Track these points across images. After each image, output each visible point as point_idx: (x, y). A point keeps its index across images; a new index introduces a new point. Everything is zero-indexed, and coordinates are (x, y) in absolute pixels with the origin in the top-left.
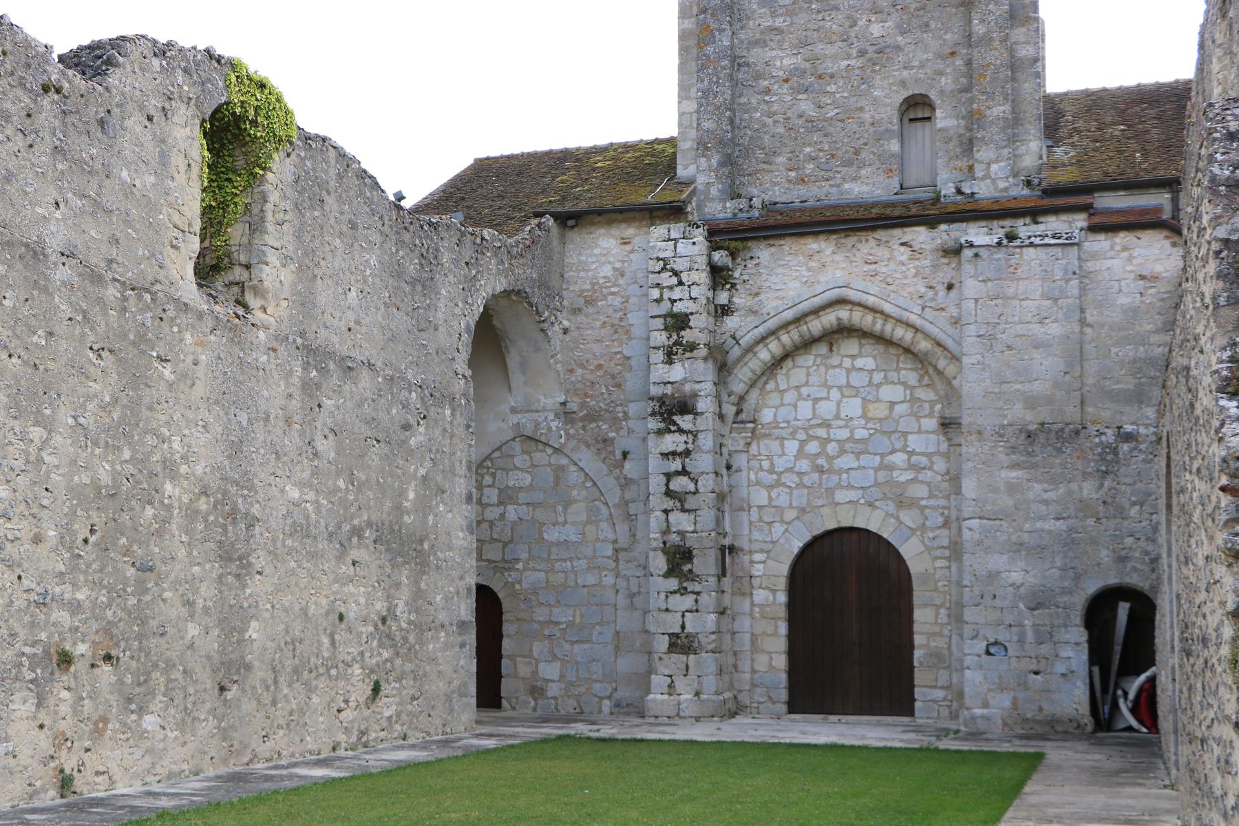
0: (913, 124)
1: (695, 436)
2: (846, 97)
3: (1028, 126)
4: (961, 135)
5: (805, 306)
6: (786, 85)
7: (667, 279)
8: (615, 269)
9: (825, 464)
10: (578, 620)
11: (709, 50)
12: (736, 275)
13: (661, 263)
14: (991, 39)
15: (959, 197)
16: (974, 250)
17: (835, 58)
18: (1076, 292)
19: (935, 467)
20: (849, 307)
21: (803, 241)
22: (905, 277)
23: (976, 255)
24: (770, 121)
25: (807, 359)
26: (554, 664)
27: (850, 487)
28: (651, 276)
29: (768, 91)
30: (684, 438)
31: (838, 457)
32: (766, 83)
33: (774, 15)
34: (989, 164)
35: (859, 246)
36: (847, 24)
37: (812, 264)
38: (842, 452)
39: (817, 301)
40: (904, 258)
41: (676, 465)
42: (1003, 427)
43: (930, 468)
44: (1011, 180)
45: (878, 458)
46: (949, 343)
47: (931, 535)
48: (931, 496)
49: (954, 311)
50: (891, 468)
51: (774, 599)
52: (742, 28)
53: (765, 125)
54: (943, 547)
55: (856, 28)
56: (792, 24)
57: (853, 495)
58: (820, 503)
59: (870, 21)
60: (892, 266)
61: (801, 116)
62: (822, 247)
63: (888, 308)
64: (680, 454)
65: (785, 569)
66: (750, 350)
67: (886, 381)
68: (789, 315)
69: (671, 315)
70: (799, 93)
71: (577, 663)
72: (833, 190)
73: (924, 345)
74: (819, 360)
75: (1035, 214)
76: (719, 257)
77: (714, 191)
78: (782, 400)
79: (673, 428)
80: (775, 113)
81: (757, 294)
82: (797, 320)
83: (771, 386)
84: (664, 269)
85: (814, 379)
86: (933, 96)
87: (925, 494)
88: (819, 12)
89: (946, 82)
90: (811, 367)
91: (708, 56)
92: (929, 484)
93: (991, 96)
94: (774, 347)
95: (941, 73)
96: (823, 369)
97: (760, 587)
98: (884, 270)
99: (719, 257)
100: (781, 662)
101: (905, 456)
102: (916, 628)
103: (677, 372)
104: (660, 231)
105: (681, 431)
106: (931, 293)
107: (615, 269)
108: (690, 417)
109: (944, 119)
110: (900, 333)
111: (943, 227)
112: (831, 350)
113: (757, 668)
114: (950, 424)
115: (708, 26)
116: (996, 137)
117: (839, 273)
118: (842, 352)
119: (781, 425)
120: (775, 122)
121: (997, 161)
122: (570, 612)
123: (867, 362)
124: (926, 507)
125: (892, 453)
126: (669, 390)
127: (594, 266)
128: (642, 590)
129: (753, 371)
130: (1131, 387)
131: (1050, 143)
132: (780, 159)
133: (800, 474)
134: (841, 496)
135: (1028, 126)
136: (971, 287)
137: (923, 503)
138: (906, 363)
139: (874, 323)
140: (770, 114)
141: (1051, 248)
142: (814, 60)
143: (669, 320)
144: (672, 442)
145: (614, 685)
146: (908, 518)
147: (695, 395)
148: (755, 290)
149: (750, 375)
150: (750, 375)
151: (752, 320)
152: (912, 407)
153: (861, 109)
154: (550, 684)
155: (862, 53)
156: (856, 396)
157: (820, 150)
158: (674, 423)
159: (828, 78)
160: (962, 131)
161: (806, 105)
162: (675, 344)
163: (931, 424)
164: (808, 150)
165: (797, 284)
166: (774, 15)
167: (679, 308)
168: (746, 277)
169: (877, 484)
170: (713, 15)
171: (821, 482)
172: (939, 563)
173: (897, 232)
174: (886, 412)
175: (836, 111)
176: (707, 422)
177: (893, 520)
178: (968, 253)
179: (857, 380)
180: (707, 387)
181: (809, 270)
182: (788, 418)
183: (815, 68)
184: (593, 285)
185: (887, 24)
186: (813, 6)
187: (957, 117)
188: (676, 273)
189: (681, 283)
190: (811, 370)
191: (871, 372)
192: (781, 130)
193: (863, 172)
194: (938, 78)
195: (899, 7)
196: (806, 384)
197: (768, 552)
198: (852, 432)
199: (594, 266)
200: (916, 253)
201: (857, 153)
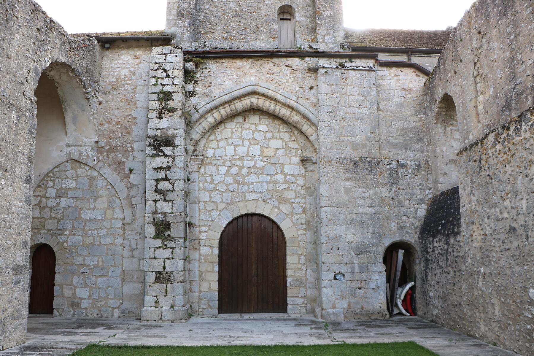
0: (282, 21)
1: (174, 158)
2: (252, 3)
5: (235, 94)
7: (160, 74)
8: (130, 71)
9: (241, 180)
10: (100, 264)
13: (158, 65)
16: (325, 70)
18: (375, 93)
19: (298, 182)
20: (257, 97)
21: (234, 61)
22: (288, 82)
23: (326, 72)
24: (214, 10)
25: (231, 125)
26: (85, 289)
27: (254, 192)
28: (151, 72)
30: (167, 159)
31: (247, 176)
37: (239, 73)
38: (250, 173)
39: (242, 92)
40: (288, 72)
41: (162, 175)
42: (341, 159)
43: (296, 183)
44: (334, 44)
45: (269, 177)
46: (311, 117)
47: (296, 217)
48: (296, 197)
49: (314, 100)
50: (275, 182)
51: (212, 252)
53: (212, 11)
54: (302, 224)
57: (255, 196)
58: (238, 200)
60: (281, 76)
63: (279, 97)
64: (164, 169)
65: (218, 236)
66: (203, 116)
67: (273, 137)
68: (226, 98)
69: (162, 92)
71: (99, 288)
72: (246, 44)
74: (238, 125)
75: (351, 57)
76: (190, 65)
77: (186, 37)
78: (218, 145)
79: (161, 154)
80: (217, 7)
81: (209, 87)
82: (230, 102)
83: (212, 137)
84: (159, 68)
85: (235, 135)
86: (294, 6)
87: (293, 196)
90: (234, 129)
92: (295, 191)
94: (216, 116)
96: (240, 130)
97: (205, 245)
98: (277, 78)
99: (190, 65)
100: (215, 286)
101: (283, 176)
102: (288, 266)
103: (164, 123)
104: (156, 50)
105: (165, 155)
107: (130, 71)
108: (171, 148)
109: (299, 16)
110: (284, 112)
111: (307, 59)
112: (245, 121)
113: (202, 289)
114: (306, 160)
117: (253, 78)
118: (250, 122)
119: (217, 158)
120: (217, 10)
121: (328, 35)
122: (96, 259)
123: (263, 128)
124: (294, 203)
125: (276, 174)
126: (159, 133)
127: (118, 70)
128: (138, 246)
129: (204, 128)
130: (402, 141)
133: (227, 184)
134: (249, 196)
136: (324, 88)
137: (292, 200)
138: (283, 128)
139: (270, 105)
141: (362, 72)
143: (160, 95)
144: (160, 161)
145: (121, 301)
146: (284, 208)
147: (174, 136)
148: (207, 84)
149: (202, 130)
150: (202, 130)
151: (206, 100)
152: (286, 152)
153: (260, 9)
154: (83, 301)
156: (257, 144)
158: (162, 151)
162: (163, 108)
163: (297, 160)
164: (233, 24)
165: (231, 83)
167: (166, 89)
168: (203, 78)
169: (268, 191)
171: (238, 188)
172: (301, 232)
173: (284, 60)
174: (273, 154)
175: (248, 8)
176: (179, 151)
177: (276, 210)
178: (321, 71)
179: (257, 136)
180: (181, 132)
181: (237, 76)
182: (221, 155)
184: (117, 79)
188: (165, 71)
189: (168, 76)
190: (234, 130)
193: (261, 37)
196: (231, 137)
197: (209, 226)
198: (255, 163)
199: (118, 70)
201: (258, 28)
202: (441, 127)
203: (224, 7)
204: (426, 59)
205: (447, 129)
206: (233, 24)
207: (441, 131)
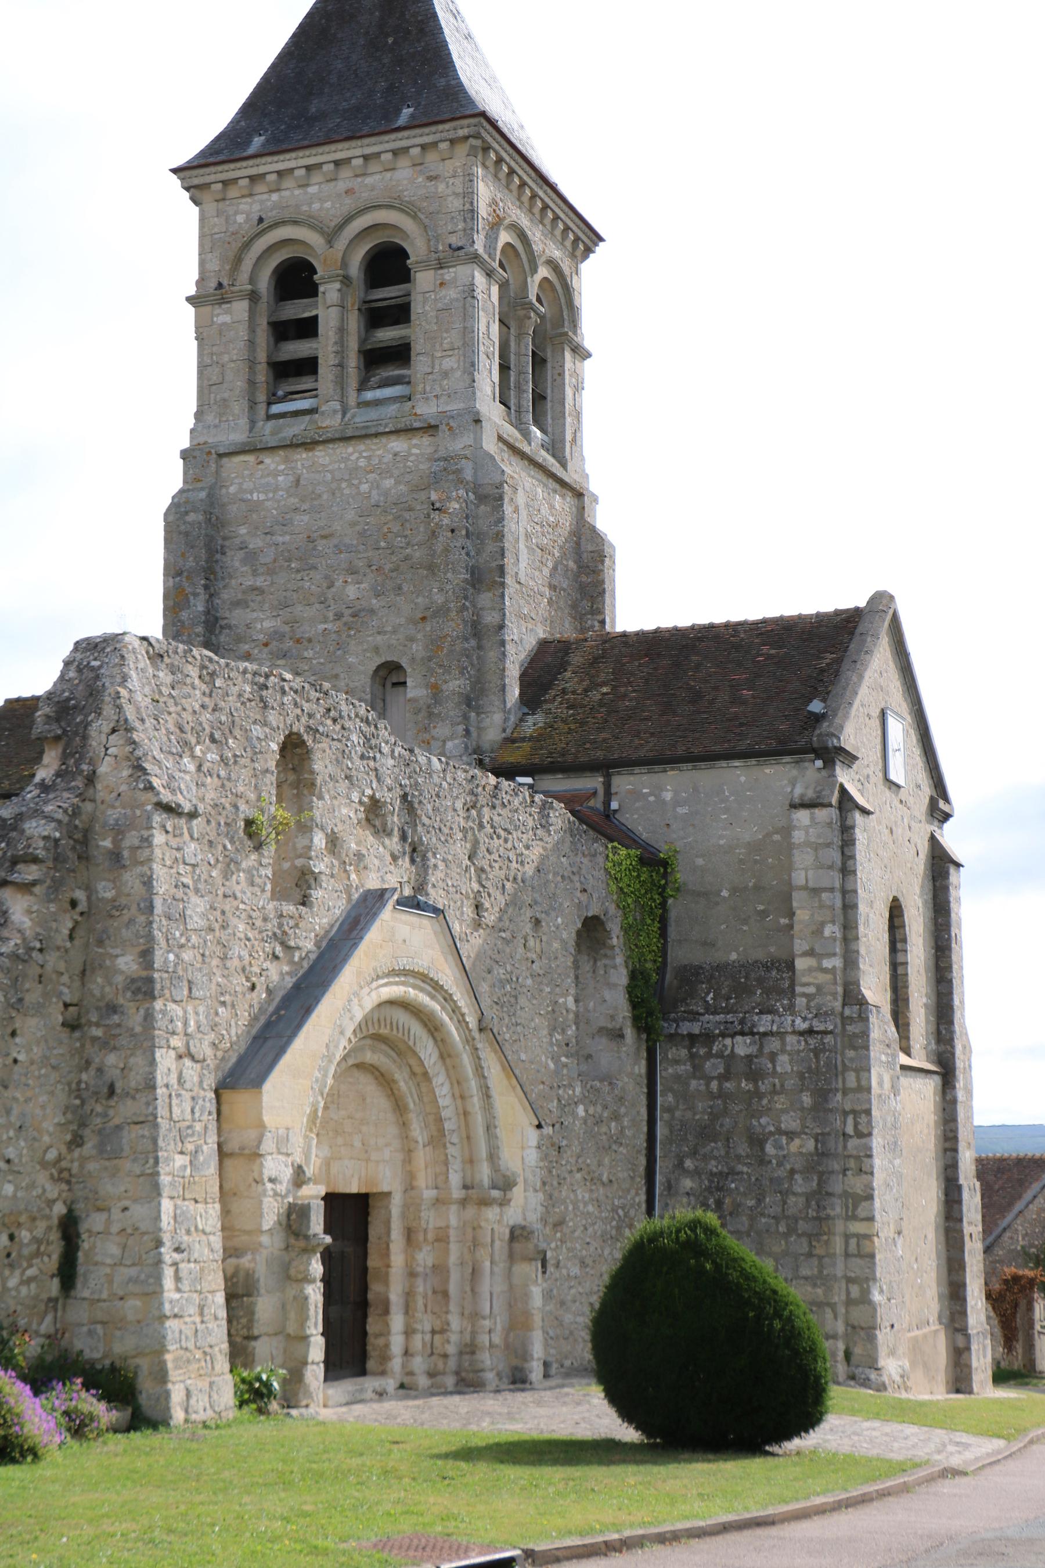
2: (322, 664)
3: (492, 697)
6: (266, 650)
11: (184, 615)
14: (449, 610)
32: (247, 647)
33: (255, 573)
34: (444, 742)
36: (325, 585)
52: (225, 587)
55: (333, 590)
56: (272, 583)
59: (346, 582)
88: (298, 571)
89: (418, 649)
91: (183, 622)
93: (447, 670)
95: (412, 639)
109: (415, 689)
115: (184, 590)
116: (452, 713)
121: (451, 738)
131: (526, 710)
135: (492, 697)
142: (292, 622)
155: (339, 616)
159: (305, 643)
170: (188, 578)
183: (293, 631)
185: (362, 586)
186: (293, 565)
187: (427, 686)
194: (409, 644)
195: (374, 568)
202: (588, 961)
204: (645, 777)
205: (599, 963)
207: (587, 969)
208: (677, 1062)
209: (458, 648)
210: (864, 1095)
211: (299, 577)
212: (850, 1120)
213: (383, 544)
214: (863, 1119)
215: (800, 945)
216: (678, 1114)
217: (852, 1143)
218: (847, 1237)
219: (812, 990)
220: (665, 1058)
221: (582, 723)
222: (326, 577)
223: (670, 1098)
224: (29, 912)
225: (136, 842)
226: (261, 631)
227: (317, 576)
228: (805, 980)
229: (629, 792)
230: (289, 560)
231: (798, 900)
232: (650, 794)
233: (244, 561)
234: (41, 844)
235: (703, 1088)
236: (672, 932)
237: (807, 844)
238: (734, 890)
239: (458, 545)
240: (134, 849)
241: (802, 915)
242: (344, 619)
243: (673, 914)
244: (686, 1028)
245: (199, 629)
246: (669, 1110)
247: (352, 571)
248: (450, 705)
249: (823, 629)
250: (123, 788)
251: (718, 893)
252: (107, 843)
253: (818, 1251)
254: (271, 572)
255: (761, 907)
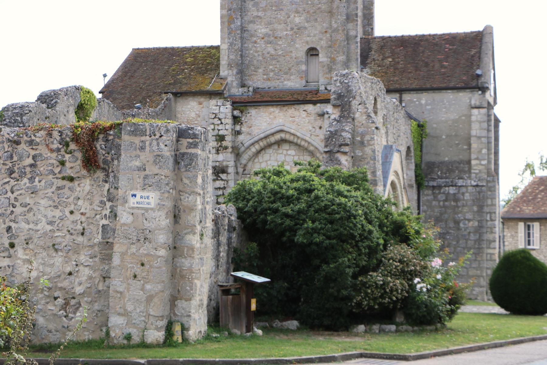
0: (312, 57)
1: (227, 182)
3: (353, 62)
4: (328, 65)
5: (268, 133)
6: (263, 40)
7: (217, 121)
8: (196, 114)
11: (232, 26)
12: (243, 119)
13: (214, 115)
14: (339, 30)
15: (326, 91)
16: (329, 115)
17: (282, 31)
21: (268, 107)
22: (305, 123)
24: (256, 54)
25: (270, 151)
28: (211, 120)
29: (255, 42)
30: (223, 182)
32: (255, 39)
33: (258, 10)
35: (288, 110)
36: (286, 17)
37: (271, 116)
39: (273, 131)
40: (304, 116)
41: (220, 192)
52: (245, 15)
53: (254, 56)
55: (290, 19)
56: (265, 15)
60: (300, 119)
61: (268, 53)
62: (275, 111)
63: (298, 134)
64: (222, 188)
66: (248, 148)
68: (262, 136)
69: (218, 135)
70: (268, 44)
72: (280, 84)
73: (311, 148)
74: (274, 151)
76: (236, 113)
77: (235, 84)
79: (219, 179)
80: (258, 52)
81: (251, 127)
82: (266, 137)
83: (256, 160)
84: (215, 117)
85: (272, 158)
86: (318, 48)
88: (276, 11)
91: (232, 29)
93: (338, 53)
94: (257, 147)
95: (321, 39)
96: (276, 154)
99: (236, 113)
103: (221, 157)
104: (213, 102)
105: (222, 180)
106: (314, 129)
107: (196, 114)
108: (225, 175)
109: (322, 58)
110: (303, 143)
111: (318, 105)
112: (279, 147)
117: (281, 120)
118: (283, 148)
120: (259, 55)
126: (217, 164)
127: (188, 113)
129: (249, 156)
131: (362, 67)
132: (260, 71)
139: (294, 139)
140: (257, 52)
142: (273, 30)
143: (217, 137)
144: (219, 184)
147: (227, 167)
148: (250, 125)
149: (248, 157)
150: (248, 157)
151: (248, 137)
153: (291, 52)
155: (292, 29)
157: (276, 68)
158: (220, 177)
160: (329, 63)
161: (270, 49)
162: (220, 146)
164: (271, 67)
165: (265, 124)
166: (258, 10)
167: (221, 133)
168: (246, 120)
170: (234, 12)
173: (302, 106)
176: (231, 177)
180: (232, 163)
181: (270, 118)
184: (188, 120)
185: (301, 18)
187: (327, 57)
188: (220, 119)
189: (222, 123)
191: (293, 156)
192: (260, 58)
193: (292, 77)
196: (270, 160)
199: (188, 113)
200: (309, 114)
201: (290, 69)
203: (264, 52)
204: (415, 95)
206: (271, 67)
208: (428, 195)
209: (342, 44)
210: (493, 207)
211: (276, 13)
212: (488, 215)
213: (310, 2)
214: (493, 215)
215: (473, 156)
216: (428, 213)
217: (489, 223)
218: (487, 254)
219: (477, 171)
220: (423, 194)
221: (386, 73)
222: (287, 14)
223: (425, 208)
224: (347, 160)
225: (369, 139)
226: (261, 33)
227: (283, 13)
228: (475, 168)
229: (409, 100)
230: (272, 6)
231: (473, 140)
232: (417, 101)
233: (253, 6)
234: (349, 140)
235: (437, 204)
236: (424, 150)
237: (477, 121)
238: (447, 136)
239: (343, 5)
240: (368, 141)
241: (474, 146)
242: (294, 30)
243: (424, 144)
244: (431, 183)
245: (239, 32)
246: (425, 211)
247: (297, 12)
248: (339, 65)
249: (468, 39)
250: (364, 122)
251: (441, 137)
252: (359, 139)
253: (479, 259)
254: (264, 10)
255: (457, 142)
